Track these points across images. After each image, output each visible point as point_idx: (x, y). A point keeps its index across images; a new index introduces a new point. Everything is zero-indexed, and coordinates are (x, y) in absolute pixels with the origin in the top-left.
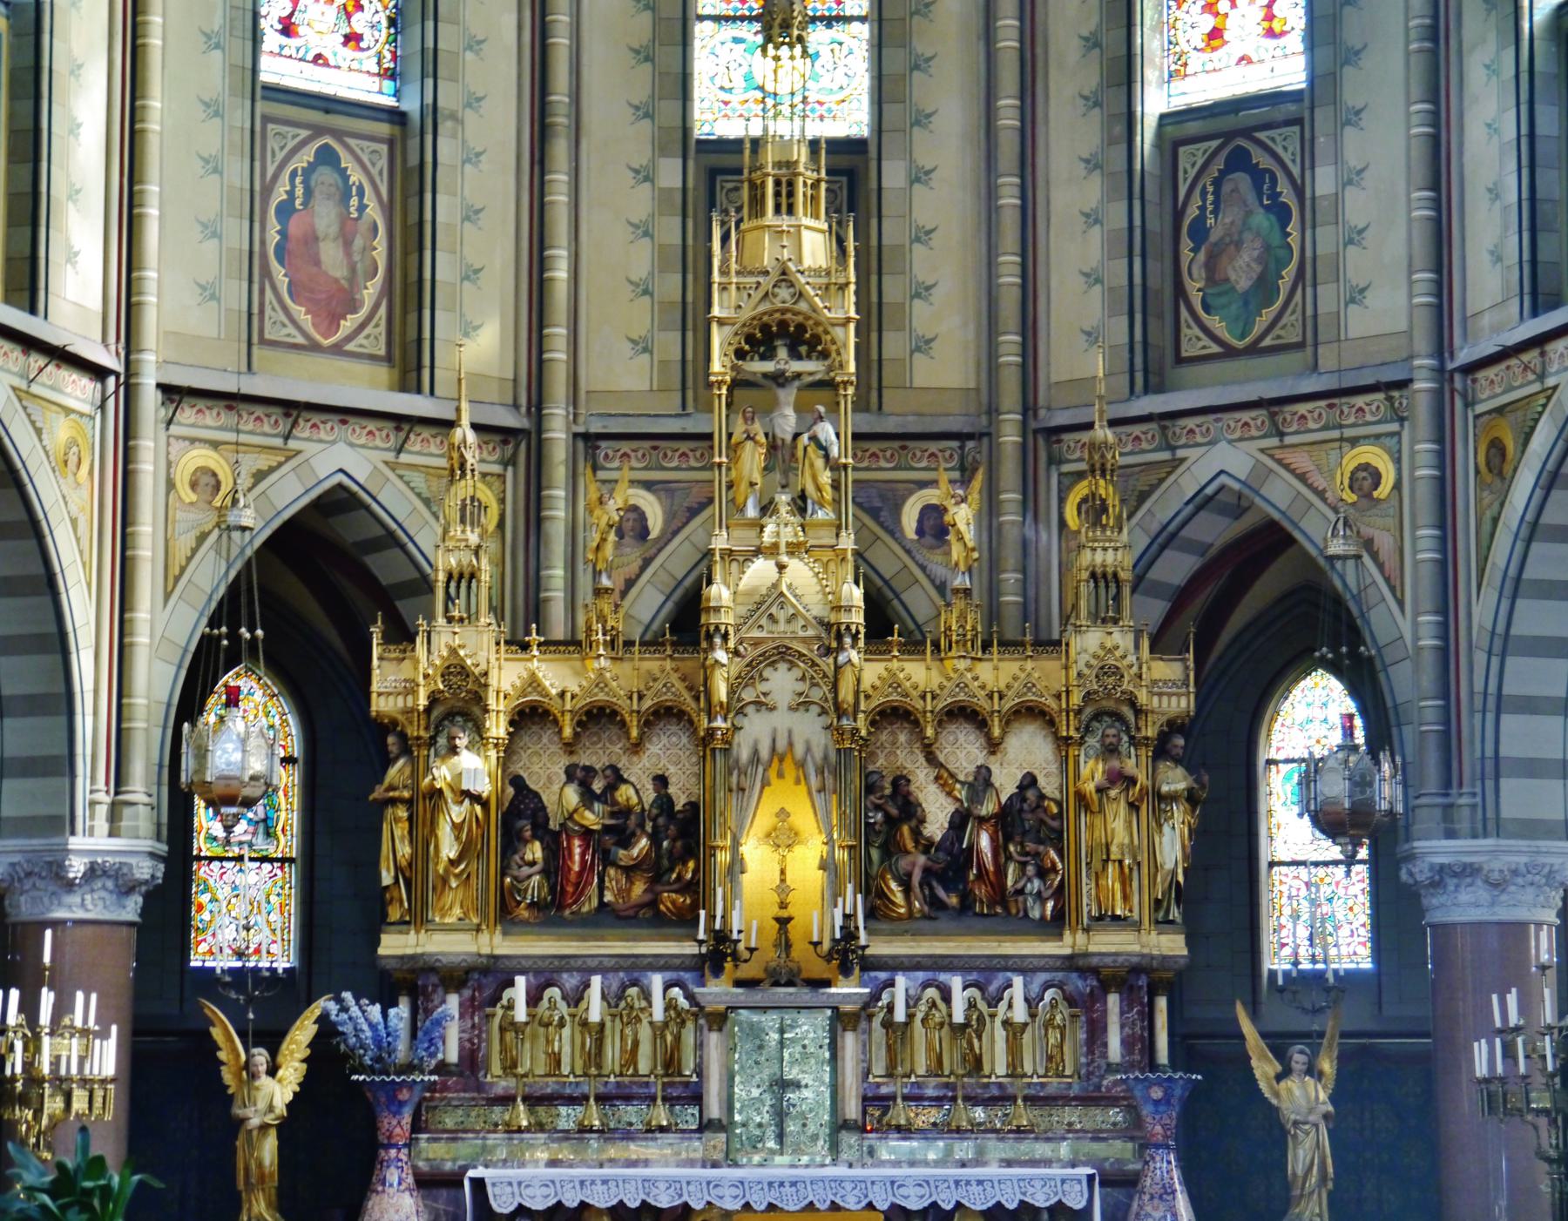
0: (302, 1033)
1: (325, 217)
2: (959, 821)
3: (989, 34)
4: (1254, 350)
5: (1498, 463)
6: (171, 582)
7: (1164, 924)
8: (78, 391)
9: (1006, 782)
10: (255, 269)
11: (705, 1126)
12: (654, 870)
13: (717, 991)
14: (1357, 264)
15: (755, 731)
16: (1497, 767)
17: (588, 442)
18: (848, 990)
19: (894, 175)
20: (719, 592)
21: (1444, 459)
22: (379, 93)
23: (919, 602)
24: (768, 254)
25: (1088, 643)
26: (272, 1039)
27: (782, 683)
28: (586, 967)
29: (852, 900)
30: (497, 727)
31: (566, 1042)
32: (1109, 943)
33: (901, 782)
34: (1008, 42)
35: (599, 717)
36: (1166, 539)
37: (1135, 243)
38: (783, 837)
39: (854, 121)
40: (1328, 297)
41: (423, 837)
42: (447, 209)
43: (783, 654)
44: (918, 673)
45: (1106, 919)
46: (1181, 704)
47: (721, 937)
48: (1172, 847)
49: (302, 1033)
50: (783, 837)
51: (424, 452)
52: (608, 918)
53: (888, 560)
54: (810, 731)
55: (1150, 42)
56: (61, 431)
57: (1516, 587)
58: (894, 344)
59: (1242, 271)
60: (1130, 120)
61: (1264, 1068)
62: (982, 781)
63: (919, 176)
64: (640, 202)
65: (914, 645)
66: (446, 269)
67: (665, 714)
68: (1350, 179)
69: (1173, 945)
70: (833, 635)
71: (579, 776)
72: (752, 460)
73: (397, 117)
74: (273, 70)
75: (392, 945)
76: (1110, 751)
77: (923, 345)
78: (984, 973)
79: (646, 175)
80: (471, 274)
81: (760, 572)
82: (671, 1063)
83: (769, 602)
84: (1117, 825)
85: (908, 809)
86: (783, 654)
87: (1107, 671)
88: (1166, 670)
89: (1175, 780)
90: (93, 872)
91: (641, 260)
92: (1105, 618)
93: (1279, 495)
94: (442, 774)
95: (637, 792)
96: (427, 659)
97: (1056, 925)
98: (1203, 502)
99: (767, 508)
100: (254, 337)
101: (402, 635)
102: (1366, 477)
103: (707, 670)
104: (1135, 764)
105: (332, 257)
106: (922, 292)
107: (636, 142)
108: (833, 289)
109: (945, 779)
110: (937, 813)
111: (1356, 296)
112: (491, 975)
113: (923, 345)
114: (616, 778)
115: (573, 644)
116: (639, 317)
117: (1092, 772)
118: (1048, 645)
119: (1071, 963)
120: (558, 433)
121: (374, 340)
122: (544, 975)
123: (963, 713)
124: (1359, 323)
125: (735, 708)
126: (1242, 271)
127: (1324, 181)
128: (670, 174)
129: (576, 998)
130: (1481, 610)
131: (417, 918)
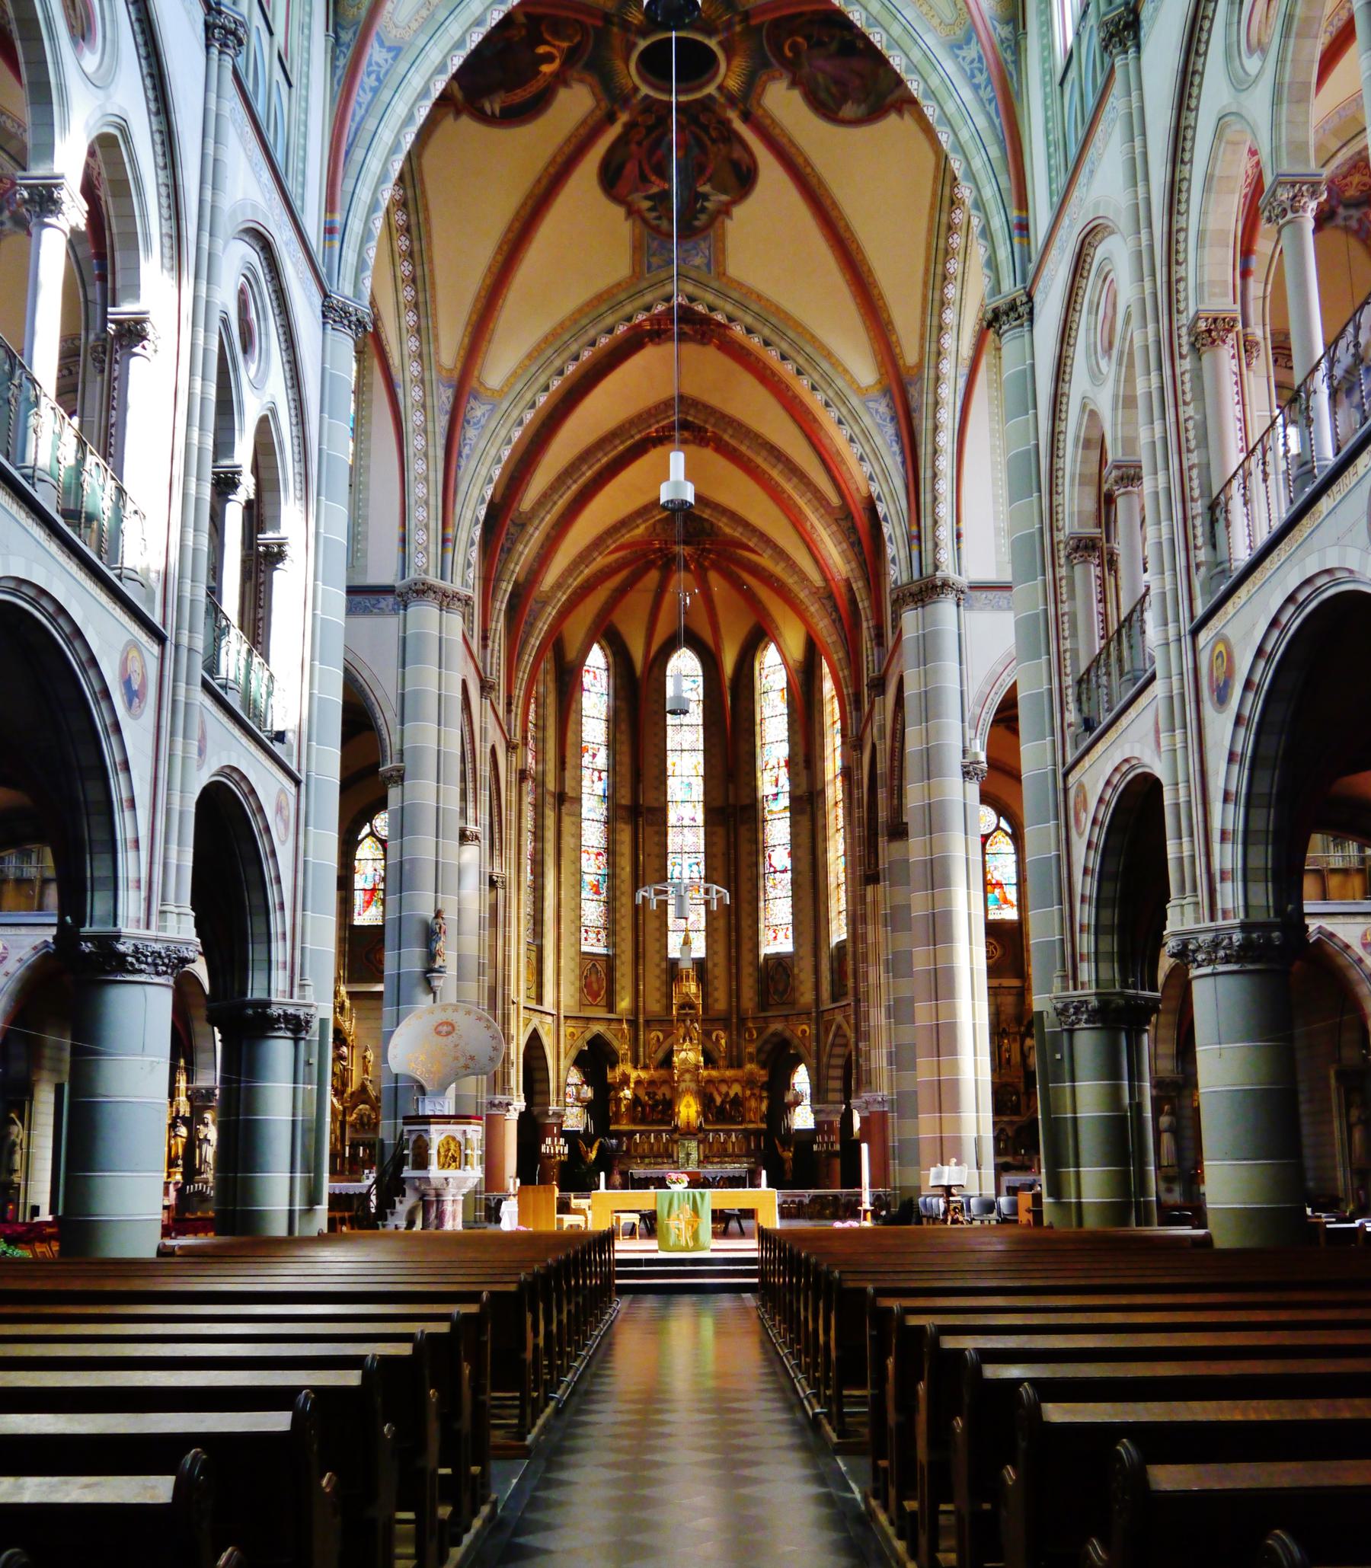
0: (596, 1145)
1: (594, 978)
2: (723, 1102)
3: (729, 936)
4: (784, 1003)
5: (827, 1031)
6: (566, 1055)
7: (762, 1121)
8: (549, 1019)
9: (732, 1094)
10: (581, 990)
11: (674, 1162)
12: (663, 1112)
13: (676, 1136)
14: (803, 988)
15: (683, 1086)
16: (827, 1091)
17: (647, 1023)
18: (701, 1136)
19: (710, 965)
20: (675, 1059)
21: (818, 1029)
22: (602, 951)
23: (716, 1055)
24: (684, 990)
25: (750, 1067)
26: (590, 1145)
27: (687, 1076)
28: (650, 1132)
29: (701, 1119)
30: (632, 1085)
31: (646, 1146)
32: (751, 1126)
33: (711, 1095)
34: (733, 938)
36: (766, 1042)
37: (759, 981)
38: (688, 1106)
40: (797, 995)
41: (618, 1106)
42: (618, 975)
43: (688, 1071)
44: (714, 1073)
45: (751, 1122)
46: (765, 1079)
47: (676, 1126)
48: (764, 1107)
49: (596, 1145)
50: (688, 1106)
51: (614, 1026)
52: (653, 1122)
53: (709, 1046)
54: (693, 1086)
55: (762, 938)
56: (546, 1027)
57: (830, 1056)
58: (710, 1001)
59: (781, 988)
60: (758, 955)
61: (780, 1150)
62: (727, 1094)
63: (715, 965)
64: (657, 971)
65: (713, 1068)
66: (618, 987)
67: (665, 1082)
68: (801, 971)
69: (764, 1126)
70: (697, 1067)
71: (648, 1094)
72: (682, 1031)
73: (607, 955)
74: (585, 948)
75: (612, 1127)
76: (751, 1089)
77: (716, 1000)
78: (728, 1133)
79: (658, 965)
80: (623, 988)
81: (683, 1055)
82: (667, 1150)
83: (685, 1061)
84: (753, 1103)
85: (712, 1099)
86: (688, 1071)
87: (751, 1073)
88: (762, 1072)
89: (765, 1094)
90: (554, 1113)
91: (657, 984)
92: (751, 1061)
93: (788, 1034)
94: (622, 1095)
95: (659, 1097)
96: (618, 1071)
97: (740, 1123)
98: (775, 1034)
99: (684, 1040)
100: (582, 1005)
101: (613, 1067)
102: (804, 1032)
103: (672, 1074)
104: (757, 1091)
105: (595, 986)
106: (716, 989)
107: (657, 959)
108: (697, 997)
109: (720, 1094)
110: (718, 1100)
111: (802, 994)
112: (632, 1133)
113: (716, 1000)
114: (655, 1094)
115: (645, 1067)
116: (657, 995)
117: (748, 1093)
118: (740, 1066)
119: (745, 1130)
120: (641, 1020)
121: (603, 1003)
122: (642, 1133)
123: (723, 1081)
125: (678, 1082)
126: (781, 988)
127: (796, 970)
128: (664, 965)
129: (648, 1137)
130: (825, 1059)
131: (617, 1122)
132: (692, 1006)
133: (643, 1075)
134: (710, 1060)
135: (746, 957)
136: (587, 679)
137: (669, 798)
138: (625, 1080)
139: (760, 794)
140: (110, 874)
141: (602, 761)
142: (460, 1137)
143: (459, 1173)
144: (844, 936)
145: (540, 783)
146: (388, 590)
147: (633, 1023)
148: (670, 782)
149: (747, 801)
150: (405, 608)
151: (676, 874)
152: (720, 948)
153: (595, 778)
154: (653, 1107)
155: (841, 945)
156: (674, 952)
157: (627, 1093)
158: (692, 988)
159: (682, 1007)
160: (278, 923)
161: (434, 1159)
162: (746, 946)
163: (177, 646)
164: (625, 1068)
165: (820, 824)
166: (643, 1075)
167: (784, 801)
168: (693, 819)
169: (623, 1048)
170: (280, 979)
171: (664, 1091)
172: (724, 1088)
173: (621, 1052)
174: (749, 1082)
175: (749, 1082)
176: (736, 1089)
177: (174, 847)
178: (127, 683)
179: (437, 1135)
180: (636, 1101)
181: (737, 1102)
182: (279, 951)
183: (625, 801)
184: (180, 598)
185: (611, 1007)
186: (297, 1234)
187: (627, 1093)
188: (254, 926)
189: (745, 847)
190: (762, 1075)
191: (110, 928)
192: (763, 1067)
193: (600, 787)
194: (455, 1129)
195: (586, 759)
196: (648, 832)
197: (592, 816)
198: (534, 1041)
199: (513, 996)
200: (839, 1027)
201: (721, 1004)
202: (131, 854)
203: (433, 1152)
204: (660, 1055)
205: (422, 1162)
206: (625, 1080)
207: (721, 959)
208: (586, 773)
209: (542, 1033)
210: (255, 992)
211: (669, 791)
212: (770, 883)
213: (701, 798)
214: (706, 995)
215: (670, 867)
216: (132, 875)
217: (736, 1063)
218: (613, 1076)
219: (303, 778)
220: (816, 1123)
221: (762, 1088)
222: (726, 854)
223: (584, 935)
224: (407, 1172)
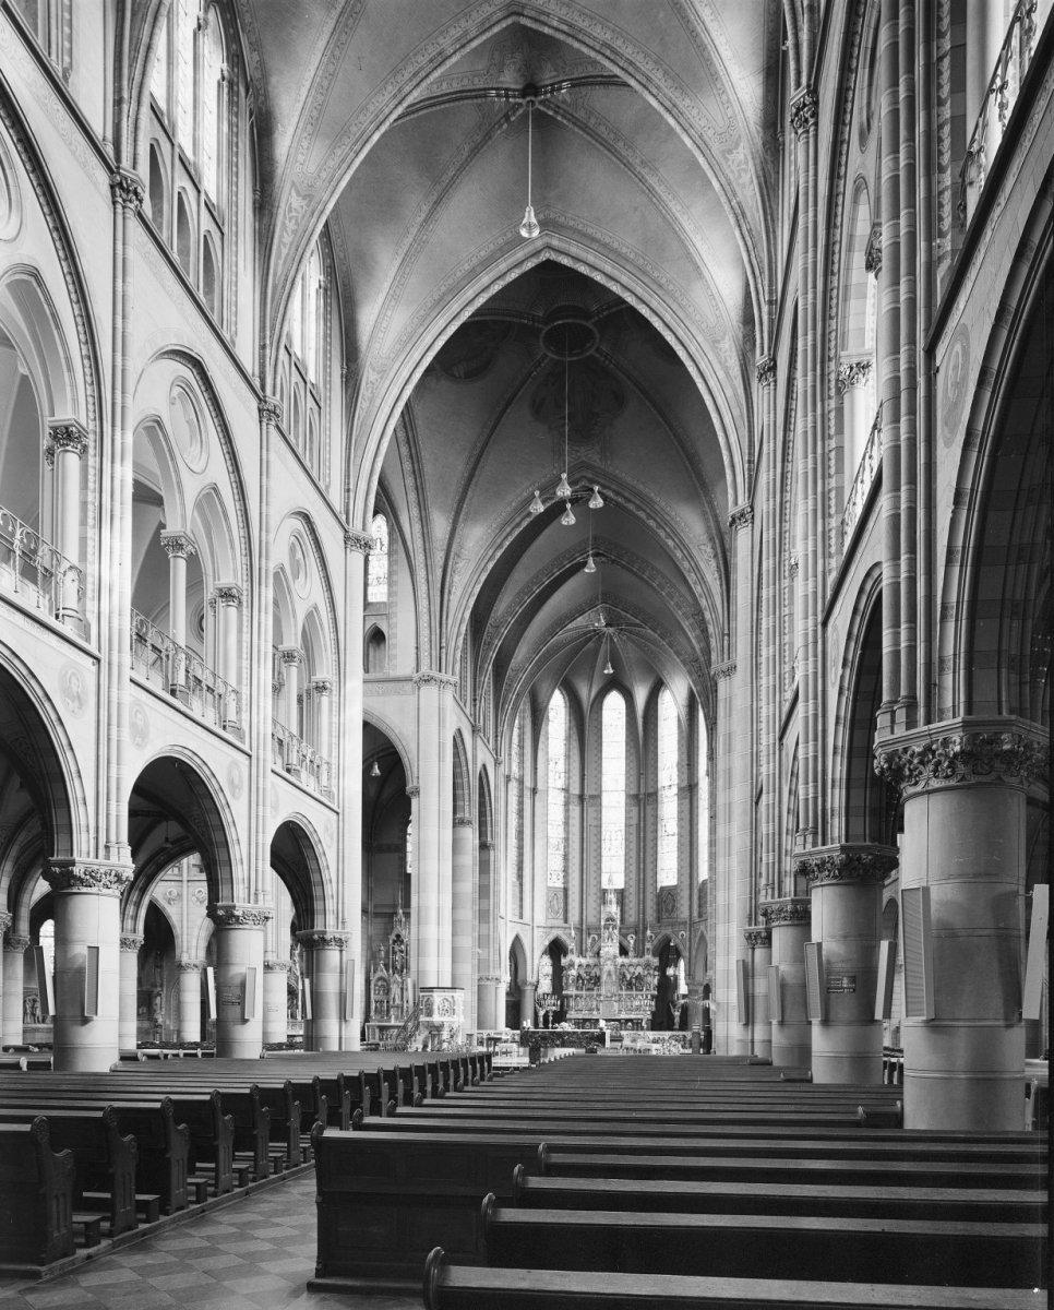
19: (626, 894)
25: (647, 956)
27: (609, 962)
34: (642, 877)
35: (588, 966)
37: (658, 904)
39: (621, 886)
41: (567, 979)
48: (656, 982)
51: (567, 931)
70: (615, 957)
72: (606, 935)
81: (606, 949)
84: (649, 979)
85: (624, 976)
89: (656, 973)
95: (593, 974)
100: (547, 918)
101: (565, 956)
104: (651, 972)
110: (628, 977)
121: (562, 917)
124: (682, 916)
132: (613, 920)
133: (584, 961)
134: (623, 951)
135: (650, 889)
136: (551, 714)
137: (603, 789)
138: (572, 965)
139: (659, 786)
140: (229, 876)
141: (561, 766)
142: (450, 999)
143: (450, 1019)
144: (706, 877)
145: (521, 782)
146: (408, 679)
147: (580, 930)
148: (604, 779)
149: (651, 790)
150: (419, 688)
151: (607, 837)
152: (633, 883)
153: (557, 777)
154: (589, 981)
155: (704, 883)
156: (605, 885)
157: (573, 972)
158: (614, 909)
159: (607, 920)
160: (330, 890)
161: (436, 1011)
162: (649, 881)
163: (258, 759)
164: (570, 957)
165: (695, 805)
166: (584, 961)
167: (675, 790)
168: (619, 802)
169: (572, 945)
170: (331, 919)
171: (595, 971)
172: (632, 970)
173: (570, 947)
174: (647, 966)
175: (647, 966)
176: (639, 970)
177: (260, 862)
178: (231, 782)
179: (437, 998)
180: (579, 976)
181: (639, 978)
182: (330, 905)
183: (575, 790)
184: (258, 734)
185: (566, 921)
186: (343, 1049)
187: (573, 972)
188: (316, 891)
189: (650, 820)
190: (655, 961)
191: (230, 903)
192: (654, 955)
193: (561, 783)
194: (448, 994)
195: (551, 765)
196: (590, 812)
197: (554, 801)
198: (517, 941)
199: (502, 913)
200: (702, 933)
201: (632, 918)
202: (239, 866)
203: (435, 1007)
204: (596, 949)
205: (430, 1014)
206: (572, 965)
207: (633, 890)
208: (551, 774)
209: (522, 936)
210: (318, 927)
211: (603, 785)
212: (664, 843)
213: (624, 788)
214: (622, 912)
215: (604, 833)
216: (241, 877)
217: (640, 954)
218: (564, 962)
219: (340, 811)
220: (689, 991)
221: (655, 970)
222: (638, 825)
223: (549, 876)
224: (423, 1018)
